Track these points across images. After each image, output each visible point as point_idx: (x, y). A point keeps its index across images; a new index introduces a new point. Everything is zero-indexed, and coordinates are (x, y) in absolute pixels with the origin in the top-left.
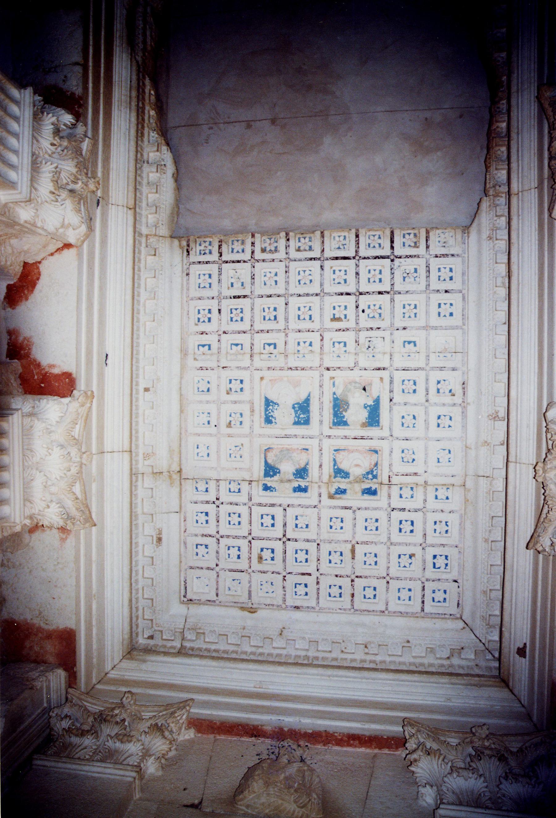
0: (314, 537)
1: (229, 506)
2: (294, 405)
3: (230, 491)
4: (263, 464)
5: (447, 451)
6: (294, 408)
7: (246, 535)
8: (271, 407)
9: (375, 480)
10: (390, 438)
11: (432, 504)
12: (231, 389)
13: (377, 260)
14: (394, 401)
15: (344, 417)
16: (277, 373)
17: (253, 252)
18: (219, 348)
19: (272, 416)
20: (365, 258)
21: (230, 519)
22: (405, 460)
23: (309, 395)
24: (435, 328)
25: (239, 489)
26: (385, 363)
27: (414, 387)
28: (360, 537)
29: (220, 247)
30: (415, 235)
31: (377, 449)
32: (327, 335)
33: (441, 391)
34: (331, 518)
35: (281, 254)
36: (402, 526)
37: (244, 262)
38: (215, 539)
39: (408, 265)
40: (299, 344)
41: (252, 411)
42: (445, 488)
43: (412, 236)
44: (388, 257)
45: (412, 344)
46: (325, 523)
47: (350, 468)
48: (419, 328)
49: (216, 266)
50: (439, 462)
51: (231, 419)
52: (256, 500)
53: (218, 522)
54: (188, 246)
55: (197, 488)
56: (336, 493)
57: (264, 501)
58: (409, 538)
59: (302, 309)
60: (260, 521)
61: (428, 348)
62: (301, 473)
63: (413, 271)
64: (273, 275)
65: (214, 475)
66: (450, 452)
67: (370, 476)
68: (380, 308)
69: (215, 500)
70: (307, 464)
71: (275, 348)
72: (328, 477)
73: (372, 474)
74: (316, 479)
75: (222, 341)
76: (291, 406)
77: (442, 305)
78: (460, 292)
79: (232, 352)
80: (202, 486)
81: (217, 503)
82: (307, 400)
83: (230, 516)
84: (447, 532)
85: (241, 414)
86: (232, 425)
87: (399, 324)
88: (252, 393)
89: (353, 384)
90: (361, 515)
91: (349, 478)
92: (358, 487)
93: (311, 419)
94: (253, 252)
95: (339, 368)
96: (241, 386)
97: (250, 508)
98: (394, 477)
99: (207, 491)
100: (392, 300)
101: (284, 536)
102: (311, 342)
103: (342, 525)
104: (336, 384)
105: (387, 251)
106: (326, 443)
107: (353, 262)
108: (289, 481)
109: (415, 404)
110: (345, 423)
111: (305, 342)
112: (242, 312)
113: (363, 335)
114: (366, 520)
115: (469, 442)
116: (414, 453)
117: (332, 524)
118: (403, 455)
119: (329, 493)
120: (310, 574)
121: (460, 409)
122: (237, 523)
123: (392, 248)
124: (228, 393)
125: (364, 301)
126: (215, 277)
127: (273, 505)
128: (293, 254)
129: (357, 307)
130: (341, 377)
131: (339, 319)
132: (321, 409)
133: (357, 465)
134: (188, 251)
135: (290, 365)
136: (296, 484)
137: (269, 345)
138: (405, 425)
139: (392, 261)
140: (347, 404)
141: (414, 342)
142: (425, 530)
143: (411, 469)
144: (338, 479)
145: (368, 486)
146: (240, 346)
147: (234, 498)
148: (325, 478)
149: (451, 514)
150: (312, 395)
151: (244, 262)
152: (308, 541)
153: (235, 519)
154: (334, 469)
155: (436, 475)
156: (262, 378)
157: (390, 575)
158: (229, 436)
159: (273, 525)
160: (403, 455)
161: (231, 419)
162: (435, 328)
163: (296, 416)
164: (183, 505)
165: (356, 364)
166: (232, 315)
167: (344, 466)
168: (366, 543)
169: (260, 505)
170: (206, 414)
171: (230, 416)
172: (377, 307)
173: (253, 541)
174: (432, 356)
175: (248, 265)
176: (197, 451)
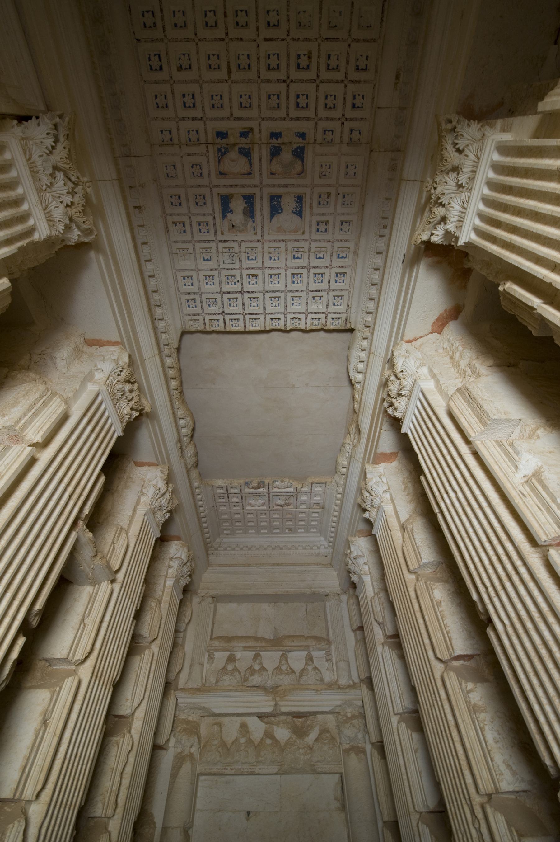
2: (282, 212)
3: (332, 131)
4: (305, 159)
5: (170, 175)
6: (282, 210)
8: (298, 210)
9: (219, 147)
10: (211, 186)
12: (326, 225)
13: (232, 312)
14: (212, 217)
15: (246, 203)
16: (293, 237)
17: (306, 318)
18: (331, 256)
19: (297, 202)
20: (240, 314)
21: (334, 102)
22: (198, 167)
24: (192, 270)
26: (221, 245)
27: (200, 227)
29: (326, 322)
30: (212, 326)
32: (260, 265)
34: (250, 107)
35: (289, 316)
37: (312, 313)
38: (349, 78)
39: (213, 309)
40: (278, 259)
41: (311, 207)
43: (214, 326)
44: (226, 314)
45: (206, 259)
48: (202, 270)
49: (330, 310)
51: (327, 200)
52: (311, 124)
53: (345, 98)
54: (346, 323)
55: (360, 133)
56: (248, 133)
59: (276, 282)
61: (195, 256)
62: (275, 152)
63: (211, 305)
64: (295, 304)
67: (223, 150)
68: (228, 283)
69: (346, 123)
70: (271, 160)
73: (222, 153)
75: (329, 261)
76: (284, 211)
77: (190, 284)
78: (181, 293)
79: (324, 253)
81: (343, 120)
82: (272, 216)
86: (327, 194)
87: (215, 273)
89: (241, 229)
90: (225, 113)
91: (239, 149)
92: (231, 140)
93: (269, 200)
94: (306, 318)
95: (251, 242)
97: (316, 115)
98: (204, 152)
99: (352, 131)
100: (221, 288)
101: (288, 86)
103: (241, 100)
104: (253, 228)
105: (227, 318)
106: (256, 181)
107: (246, 312)
108: (284, 144)
109: (197, 215)
110: (245, 197)
111: (275, 260)
112: (315, 280)
113: (237, 265)
116: (193, 173)
117: (249, 101)
119: (253, 133)
120: (266, 40)
123: (224, 320)
124: (328, 221)
125: (238, 287)
126: (331, 304)
127: (298, 119)
128: (282, 317)
129: (242, 284)
131: (254, 275)
132: (262, 210)
134: (346, 320)
136: (280, 141)
137: (298, 258)
138: (202, 197)
140: (244, 214)
141: (204, 260)
142: (174, 98)
144: (247, 147)
145: (225, 141)
146: (318, 257)
147: (330, 125)
148: (256, 148)
150: (269, 220)
151: (312, 313)
152: (268, 81)
156: (303, 233)
157: (195, 44)
158: (329, 186)
159: (298, 97)
160: (200, 171)
161: (327, 200)
162: (192, 270)
165: (240, 245)
166: (321, 278)
167: (243, 160)
169: (308, 119)
170: (346, 203)
171: (328, 202)
172: (230, 283)
173: (315, 78)
174: (191, 251)
175: (309, 311)
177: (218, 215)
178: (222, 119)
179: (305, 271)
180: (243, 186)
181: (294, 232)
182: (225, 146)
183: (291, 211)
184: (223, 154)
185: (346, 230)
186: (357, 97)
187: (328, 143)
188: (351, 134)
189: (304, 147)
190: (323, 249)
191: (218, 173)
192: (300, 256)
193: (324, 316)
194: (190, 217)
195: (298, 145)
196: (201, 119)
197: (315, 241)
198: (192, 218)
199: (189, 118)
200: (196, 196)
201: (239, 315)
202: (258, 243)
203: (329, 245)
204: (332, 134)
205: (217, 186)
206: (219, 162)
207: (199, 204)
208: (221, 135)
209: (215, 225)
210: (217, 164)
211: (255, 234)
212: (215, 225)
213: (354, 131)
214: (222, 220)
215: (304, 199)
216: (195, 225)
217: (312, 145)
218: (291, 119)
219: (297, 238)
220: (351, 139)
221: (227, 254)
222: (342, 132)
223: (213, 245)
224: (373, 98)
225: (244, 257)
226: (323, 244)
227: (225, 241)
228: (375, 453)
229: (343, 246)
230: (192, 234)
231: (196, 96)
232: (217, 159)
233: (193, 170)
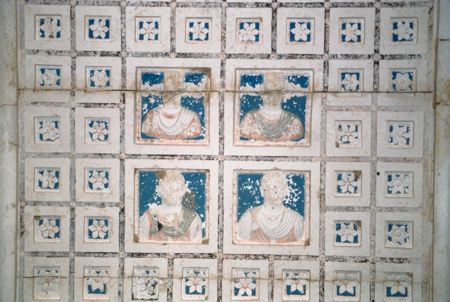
0: (230, 10)
1: (358, 52)
2: (262, 203)
3: (358, 75)
4: (307, 118)
5: (45, 137)
6: (262, 200)
7: (333, 10)
8: (295, 200)
9: (146, 96)
10: (123, 155)
11: (65, 63)
12: (355, 228)
14: (118, 210)
15: (190, 186)
16: (285, 251)
18: (372, 290)
19: (293, 187)
21: (358, 33)
22: (103, 125)
23: (239, 217)
25: (343, 78)
26: (130, 263)
27: (92, 228)
31: (142, 141)
33: (54, 223)
34: (207, 39)
36: (106, 29)
40: (254, 293)
41: (322, 195)
42: (47, 87)
45: (94, 288)
46: (215, 32)
47: (180, 113)
50: (56, 123)
52: (317, 64)
53: (377, 28)
55: (411, 77)
57: (305, 63)
60: (312, 31)
62: (250, 105)
65: (383, 100)
66: (41, 137)
67: (152, 101)
69: (381, 62)
70: (242, 118)
71: (289, 288)
72: (212, 100)
73: (150, 105)
74: (228, 98)
76: (266, 203)
79: (354, 284)
80: (402, 80)
81: (377, 57)
82: (242, 210)
83: (359, 37)
84: (42, 22)
85: (339, 190)
86: (353, 175)
88: (322, 222)
91: (182, 99)
92: (169, 84)
93: (236, 182)
95: (195, 257)
96: (339, 233)
97: (326, 51)
98: (117, 101)
99: (395, 74)
101: (275, 11)
102: (236, 294)
103: (192, 30)
104: (200, 233)
106: (214, 150)
108: (267, 92)
109: (89, 204)
110: (188, 176)
111: (245, 294)
114: (156, 37)
115: (14, 152)
116: (91, 135)
117: (206, 31)
118: (106, 132)
119: (210, 76)
121: (27, 197)
122: (348, 26)
124: (359, 222)
127: (292, 56)
130: (193, 244)
132: (221, 198)
133: (170, 117)
135: (266, 262)
136: (258, 87)
137: (297, 292)
138: (103, 174)
140: (184, 204)
142: (73, 25)
143: (93, 113)
144: (197, 96)
146: (342, 290)
148: (215, 99)
149: (36, 49)
150: (235, 218)
153: (350, 32)
154: (203, 111)
155: (58, 105)
156: (308, 243)
158: (357, 159)
159: (292, 26)
160: (106, 132)
161: (355, 184)
163: (258, 187)
164: (433, 52)
165: (171, 263)
167: (188, 116)
169: (311, 57)
171: (356, 188)
174: (65, 272)
176: (410, 135)
178: (156, 55)
180: (186, 157)
181: (288, 241)
182: (158, 95)
183: (280, 202)
184: (151, 107)
185: (401, 239)
186: (399, 24)
187: (351, 91)
188: (394, 78)
190: (352, 275)
191: (140, 135)
192: (301, 289)
194: (73, 209)
195: (293, 95)
196: (118, 54)
197: (332, 259)
198: (78, 210)
199: (95, 52)
200: (91, 172)
202: (211, 260)
203: (365, 268)
204: (358, 79)
205: (135, 156)
206: (144, 118)
207: (94, 186)
208: (151, 78)
209: (122, 223)
210: (140, 121)
211: (205, 242)
212: (122, 223)
213: (398, 75)
214: (137, 217)
215: (307, 182)
217: (319, 94)
218: (280, 57)
219: (295, 252)
220: (394, 86)
221: (142, 281)
222: (376, 76)
223: (114, 262)
224: (431, 27)
226: (351, 266)
227: (140, 255)
229: (397, 270)
230: (72, 239)
231: (112, 23)
232: (139, 114)
233: (92, 130)
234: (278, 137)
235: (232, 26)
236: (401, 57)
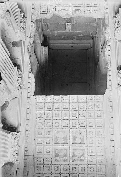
21: (46, 169)
28: (81, 173)
39: (90, 104)
41: (53, 139)
46: (71, 169)
57: (55, 163)
58: (93, 172)
67: (82, 156)
73: (83, 155)
82: (66, 137)
101: (61, 173)
103: (75, 169)
113: (80, 120)
127: (58, 164)
131: (74, 117)
136: (64, 159)
139: (86, 103)
148: (71, 157)
152: (67, 174)
155: (99, 155)
159: (58, 170)
167: (76, 153)
168: (82, 174)
169: (54, 164)
177: (85, 137)
179: (54, 118)
189: (55, 157)
193: (46, 101)
201: (80, 102)
206: (84, 153)
216: (94, 134)
225: (77, 123)
228: (21, 47)
231: (89, 170)
234: (60, 149)
235: (68, 170)
236: (39, 164)
